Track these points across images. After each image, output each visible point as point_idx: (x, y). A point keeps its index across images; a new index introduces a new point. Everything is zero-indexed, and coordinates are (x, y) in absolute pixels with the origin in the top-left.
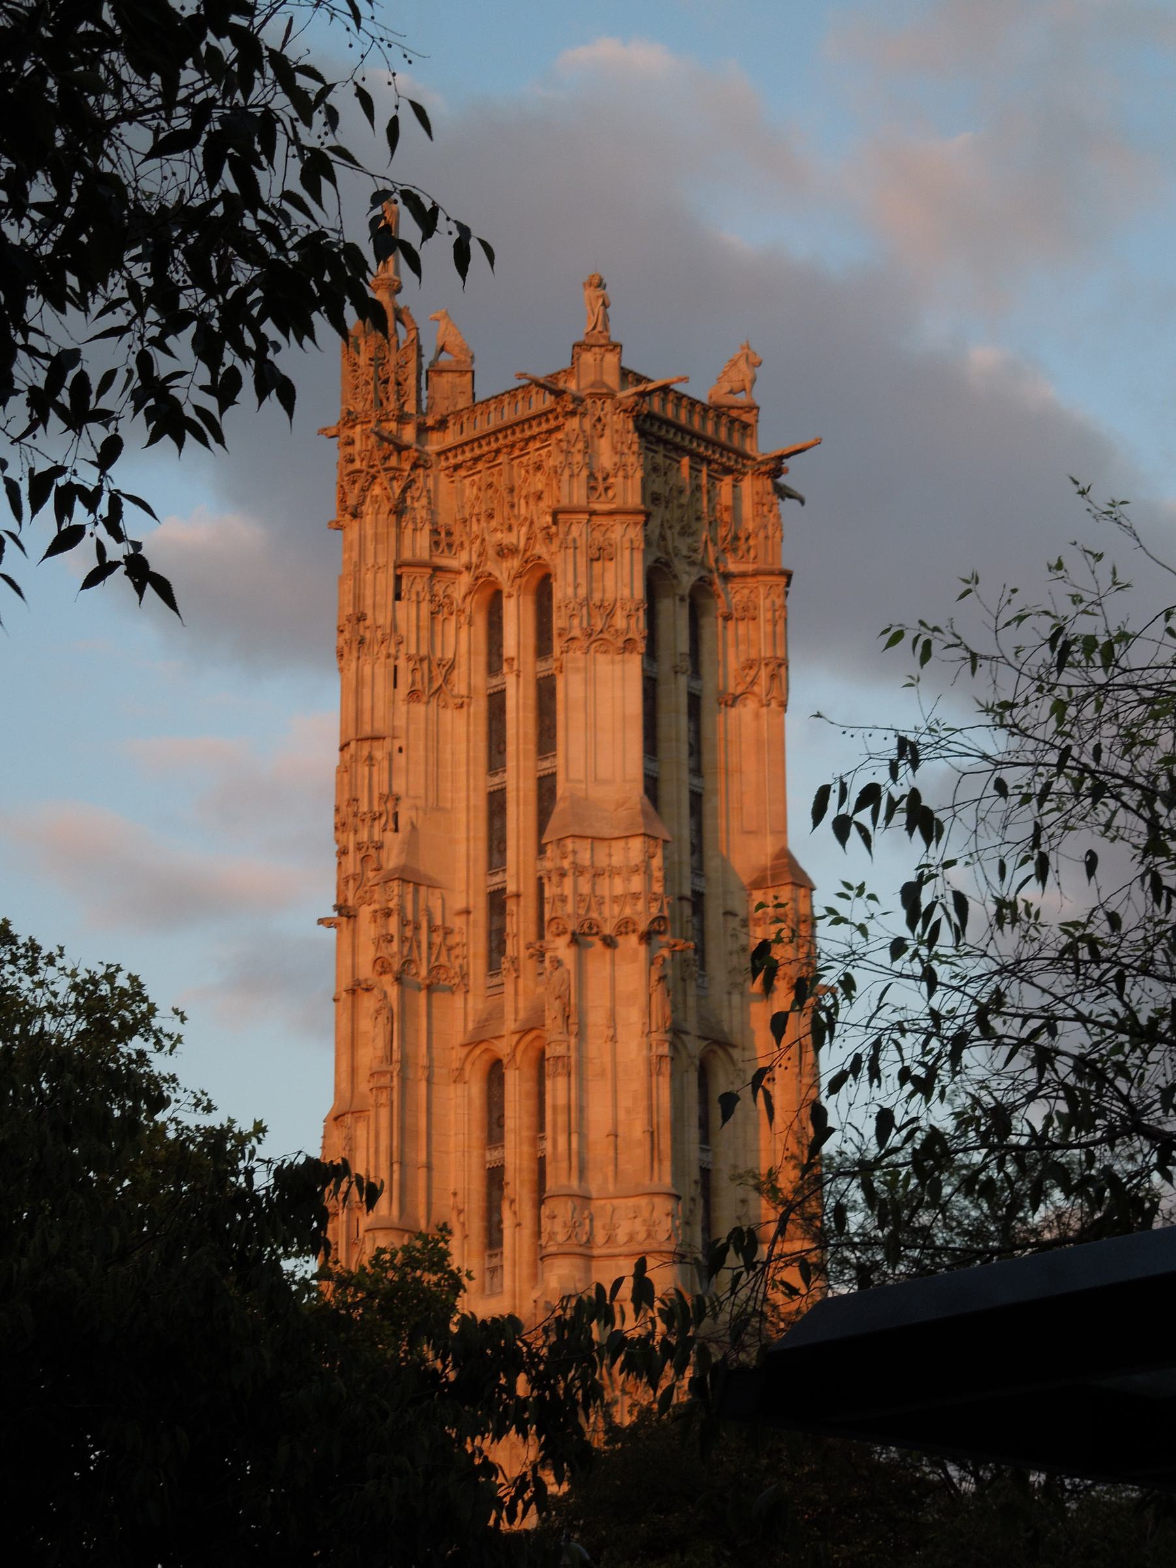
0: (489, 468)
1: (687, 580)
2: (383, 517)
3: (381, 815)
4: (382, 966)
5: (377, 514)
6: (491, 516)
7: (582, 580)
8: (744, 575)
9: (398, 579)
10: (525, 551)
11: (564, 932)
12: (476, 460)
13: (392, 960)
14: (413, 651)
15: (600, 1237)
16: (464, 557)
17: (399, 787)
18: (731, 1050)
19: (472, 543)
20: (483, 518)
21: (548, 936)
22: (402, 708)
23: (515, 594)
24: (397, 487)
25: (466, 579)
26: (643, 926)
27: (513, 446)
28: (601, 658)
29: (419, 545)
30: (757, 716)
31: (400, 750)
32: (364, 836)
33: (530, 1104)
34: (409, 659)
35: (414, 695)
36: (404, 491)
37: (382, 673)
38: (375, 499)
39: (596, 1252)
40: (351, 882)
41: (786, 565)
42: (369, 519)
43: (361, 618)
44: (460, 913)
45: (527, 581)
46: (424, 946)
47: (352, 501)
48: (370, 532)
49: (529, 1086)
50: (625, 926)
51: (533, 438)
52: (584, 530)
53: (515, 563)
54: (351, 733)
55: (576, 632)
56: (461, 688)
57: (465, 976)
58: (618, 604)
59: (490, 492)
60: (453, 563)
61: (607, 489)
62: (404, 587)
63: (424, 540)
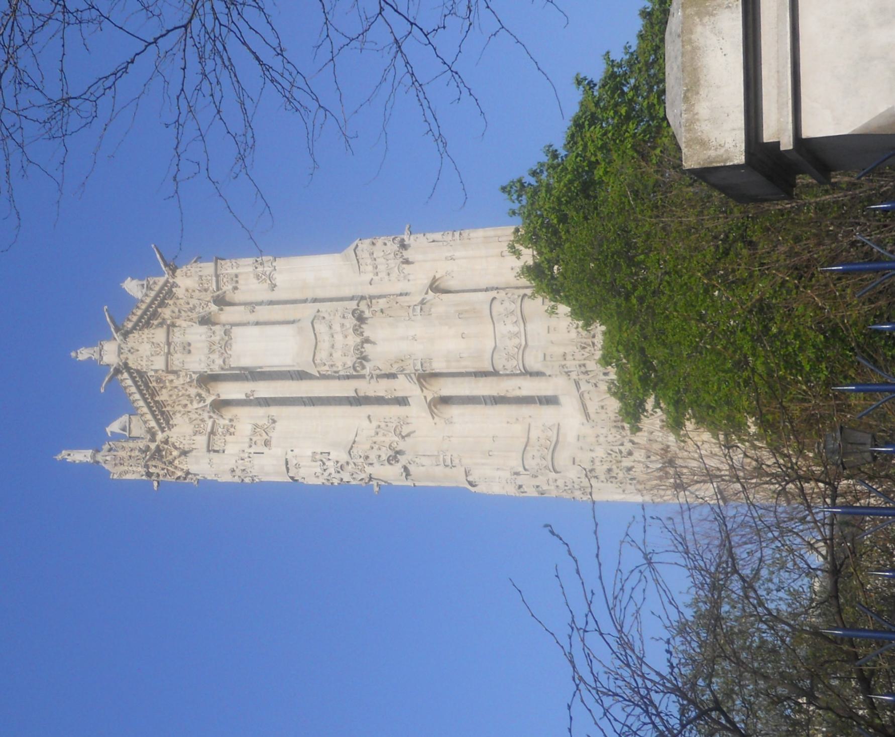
1: (214, 308)
8: (217, 282)
9: (215, 451)
11: (361, 363)
12: (163, 413)
17: (309, 453)
21: (363, 372)
24: (175, 453)
28: (234, 347)
29: (201, 440)
32: (332, 470)
34: (250, 446)
35: (267, 443)
36: (176, 448)
38: (180, 463)
44: (370, 421)
50: (357, 330)
56: (264, 422)
60: (210, 423)
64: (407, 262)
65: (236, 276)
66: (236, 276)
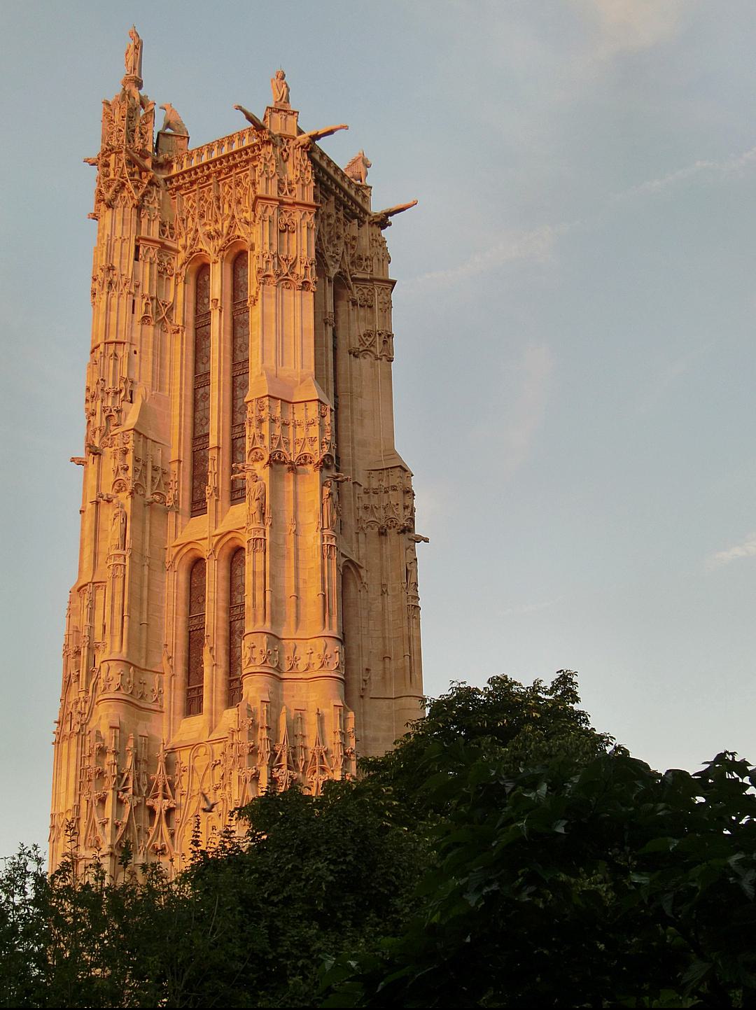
0: (201, 188)
2: (128, 210)
3: (121, 390)
4: (119, 486)
5: (124, 207)
6: (202, 216)
7: (275, 242)
8: (364, 280)
9: (137, 248)
10: (228, 234)
13: (127, 482)
14: (147, 292)
15: (286, 666)
16: (182, 241)
18: (360, 570)
19: (187, 234)
20: (196, 217)
22: (138, 327)
23: (219, 261)
25: (183, 256)
26: (317, 459)
27: (220, 173)
30: (373, 365)
31: (135, 352)
33: (224, 584)
34: (143, 297)
36: (143, 196)
37: (125, 303)
39: (284, 676)
40: (98, 432)
41: (391, 277)
42: (119, 210)
43: (111, 268)
45: (227, 254)
46: (149, 478)
47: (108, 196)
48: (119, 218)
49: (224, 572)
51: (236, 166)
52: (276, 212)
53: (220, 242)
54: (100, 340)
55: (271, 273)
56: (178, 321)
57: (176, 502)
58: (299, 260)
59: (202, 202)
61: (291, 191)
62: (141, 252)
63: (156, 228)
64: (382, 533)
65: (370, 307)
66: (370, 307)
